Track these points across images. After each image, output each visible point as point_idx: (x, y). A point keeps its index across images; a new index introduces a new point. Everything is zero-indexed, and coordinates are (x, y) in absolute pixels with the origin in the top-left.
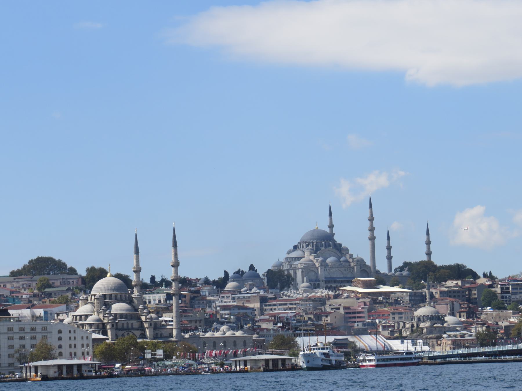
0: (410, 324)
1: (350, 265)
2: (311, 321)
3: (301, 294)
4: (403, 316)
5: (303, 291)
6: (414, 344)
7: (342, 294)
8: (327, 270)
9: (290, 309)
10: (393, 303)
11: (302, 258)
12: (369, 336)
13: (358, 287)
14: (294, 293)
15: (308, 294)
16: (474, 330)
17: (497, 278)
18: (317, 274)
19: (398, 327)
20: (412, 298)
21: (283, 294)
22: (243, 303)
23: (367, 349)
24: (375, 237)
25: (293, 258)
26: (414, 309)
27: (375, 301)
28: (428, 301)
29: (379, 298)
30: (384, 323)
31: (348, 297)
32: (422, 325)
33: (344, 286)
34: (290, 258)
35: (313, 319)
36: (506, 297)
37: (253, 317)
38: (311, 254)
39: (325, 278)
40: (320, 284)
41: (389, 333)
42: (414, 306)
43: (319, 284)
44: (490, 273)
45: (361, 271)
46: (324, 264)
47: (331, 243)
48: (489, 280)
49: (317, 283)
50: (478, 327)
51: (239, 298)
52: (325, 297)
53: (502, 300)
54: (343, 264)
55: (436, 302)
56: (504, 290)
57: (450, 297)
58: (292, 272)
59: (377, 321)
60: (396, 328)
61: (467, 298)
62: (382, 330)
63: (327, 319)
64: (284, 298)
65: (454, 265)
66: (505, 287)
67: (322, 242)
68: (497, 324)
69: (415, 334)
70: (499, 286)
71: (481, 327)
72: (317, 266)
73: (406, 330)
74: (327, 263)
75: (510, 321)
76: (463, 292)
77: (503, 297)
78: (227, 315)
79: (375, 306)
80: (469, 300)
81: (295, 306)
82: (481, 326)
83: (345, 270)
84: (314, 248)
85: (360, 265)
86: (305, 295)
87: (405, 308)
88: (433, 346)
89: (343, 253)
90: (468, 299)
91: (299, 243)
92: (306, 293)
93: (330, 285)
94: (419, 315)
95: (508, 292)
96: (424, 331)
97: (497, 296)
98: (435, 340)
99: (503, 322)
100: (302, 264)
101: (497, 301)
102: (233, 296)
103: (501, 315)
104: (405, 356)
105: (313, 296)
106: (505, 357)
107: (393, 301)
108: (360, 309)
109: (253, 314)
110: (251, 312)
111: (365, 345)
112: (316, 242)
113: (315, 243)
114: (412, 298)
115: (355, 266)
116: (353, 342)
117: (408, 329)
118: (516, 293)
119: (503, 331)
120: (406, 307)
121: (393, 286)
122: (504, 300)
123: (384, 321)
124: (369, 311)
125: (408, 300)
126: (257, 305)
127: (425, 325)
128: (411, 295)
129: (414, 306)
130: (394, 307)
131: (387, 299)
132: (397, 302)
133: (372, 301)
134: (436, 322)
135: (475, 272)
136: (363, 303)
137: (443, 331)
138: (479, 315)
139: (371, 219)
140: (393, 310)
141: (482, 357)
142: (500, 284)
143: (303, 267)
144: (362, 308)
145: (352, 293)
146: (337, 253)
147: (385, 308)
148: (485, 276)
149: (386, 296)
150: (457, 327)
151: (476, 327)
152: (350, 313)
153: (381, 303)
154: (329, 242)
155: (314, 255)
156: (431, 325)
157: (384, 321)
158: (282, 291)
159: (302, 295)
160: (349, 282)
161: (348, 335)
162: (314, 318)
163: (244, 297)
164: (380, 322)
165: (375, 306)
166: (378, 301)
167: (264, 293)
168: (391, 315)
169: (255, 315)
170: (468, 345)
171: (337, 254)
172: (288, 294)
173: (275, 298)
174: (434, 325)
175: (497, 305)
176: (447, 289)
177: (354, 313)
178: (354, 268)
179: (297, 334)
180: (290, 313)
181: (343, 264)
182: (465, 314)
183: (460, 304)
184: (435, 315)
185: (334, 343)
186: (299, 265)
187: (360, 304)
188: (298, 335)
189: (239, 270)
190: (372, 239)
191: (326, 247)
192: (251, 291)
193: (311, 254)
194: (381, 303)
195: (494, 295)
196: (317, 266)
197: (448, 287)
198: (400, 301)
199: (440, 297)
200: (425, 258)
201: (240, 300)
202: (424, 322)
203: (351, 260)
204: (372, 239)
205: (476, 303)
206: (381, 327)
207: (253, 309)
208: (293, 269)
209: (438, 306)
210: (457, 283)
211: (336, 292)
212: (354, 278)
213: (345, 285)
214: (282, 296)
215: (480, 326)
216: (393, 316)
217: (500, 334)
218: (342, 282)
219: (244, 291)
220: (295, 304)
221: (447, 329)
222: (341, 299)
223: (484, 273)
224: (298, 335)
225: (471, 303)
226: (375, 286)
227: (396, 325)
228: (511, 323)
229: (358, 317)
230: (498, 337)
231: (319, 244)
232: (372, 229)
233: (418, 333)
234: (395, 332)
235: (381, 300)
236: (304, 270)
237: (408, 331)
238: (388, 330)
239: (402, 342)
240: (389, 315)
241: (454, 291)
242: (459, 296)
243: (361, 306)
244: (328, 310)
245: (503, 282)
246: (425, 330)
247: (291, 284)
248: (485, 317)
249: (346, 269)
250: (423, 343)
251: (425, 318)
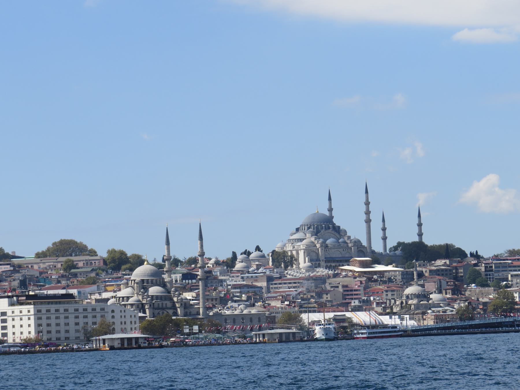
0: (400, 301)
1: (348, 246)
2: (313, 299)
3: (303, 274)
4: (395, 293)
5: (305, 271)
6: (402, 319)
7: (340, 274)
8: (327, 250)
9: (294, 287)
10: (387, 281)
11: (303, 239)
12: (364, 312)
13: (355, 266)
14: (297, 272)
15: (310, 273)
16: (458, 306)
17: (482, 258)
18: (318, 254)
19: (390, 304)
20: (404, 276)
21: (287, 273)
22: (252, 283)
23: (362, 324)
24: (371, 220)
25: (296, 239)
26: (405, 286)
27: (370, 280)
28: (416, 281)
29: (374, 276)
30: (378, 300)
31: (346, 276)
32: (410, 302)
33: (343, 266)
34: (293, 239)
35: (314, 297)
36: (490, 275)
37: (261, 294)
38: (312, 236)
39: (325, 258)
41: (382, 309)
42: (406, 284)
43: (319, 264)
44: (477, 252)
45: (358, 251)
46: (325, 246)
47: (331, 226)
48: (474, 260)
49: (318, 262)
50: (461, 303)
51: (248, 277)
52: (325, 276)
53: (486, 278)
54: (342, 245)
55: (426, 280)
56: (488, 268)
57: (439, 275)
58: (294, 253)
59: (372, 298)
60: (388, 305)
61: (454, 276)
62: (376, 307)
63: (327, 296)
64: (288, 277)
65: (444, 245)
66: (488, 266)
67: (322, 225)
68: (478, 300)
69: (404, 310)
70: (483, 265)
71: (463, 303)
72: (318, 247)
73: (397, 306)
74: (327, 244)
75: (489, 297)
76: (450, 270)
77: (486, 275)
78: (238, 293)
79: (370, 284)
80: (456, 278)
81: (299, 285)
82: (464, 302)
83: (343, 250)
84: (315, 230)
85: (357, 246)
86: (307, 274)
87: (397, 286)
88: (419, 320)
89: (342, 235)
90: (455, 277)
91: (301, 226)
92: (308, 272)
93: (329, 264)
94: (408, 294)
95: (492, 271)
96: (412, 307)
97: (481, 274)
98: (421, 315)
99: (483, 299)
100: (304, 246)
101: (480, 278)
102: (242, 275)
103: (483, 291)
104: (391, 330)
105: (314, 275)
106: (474, 330)
107: (387, 280)
108: (357, 287)
109: (261, 292)
110: (259, 291)
111: (360, 320)
112: (317, 225)
113: (316, 226)
114: (404, 276)
115: (352, 246)
116: (350, 318)
117: (398, 305)
118: (499, 271)
119: (481, 307)
120: (398, 284)
121: (387, 265)
122: (487, 278)
123: (378, 298)
124: (365, 289)
125: (401, 279)
126: (264, 284)
127: (413, 302)
128: (403, 273)
129: (406, 284)
130: (387, 285)
131: (381, 277)
132: (390, 280)
133: (367, 280)
134: (422, 299)
135: (464, 251)
136: (359, 282)
137: (429, 307)
138: (464, 292)
139: (367, 203)
140: (386, 288)
141: (455, 330)
142: (484, 263)
143: (304, 248)
144: (359, 286)
145: (350, 272)
147: (379, 285)
148: (472, 255)
149: (380, 275)
150: (440, 303)
151: (459, 303)
152: (348, 291)
153: (376, 281)
154: (328, 225)
155: (315, 237)
156: (418, 302)
157: (378, 298)
158: (286, 271)
159: (304, 274)
160: (347, 261)
161: (346, 312)
162: (316, 296)
163: (252, 277)
164: (374, 299)
165: (370, 284)
166: (373, 279)
167: (270, 272)
168: (384, 292)
169: (263, 293)
170: (449, 319)
171: (336, 236)
172: (292, 274)
173: (280, 278)
174: (420, 302)
175: (481, 282)
176: (436, 268)
177: (351, 291)
178: (351, 249)
179: (302, 311)
180: (293, 292)
181: (342, 245)
182: (450, 291)
183: (447, 282)
184: (422, 293)
185: (333, 318)
186: (301, 246)
187: (357, 283)
188: (303, 312)
189: (246, 250)
190: (368, 221)
192: (258, 271)
193: (312, 236)
194: (376, 281)
195: (479, 273)
196: (318, 247)
197: (437, 266)
198: (393, 279)
199: (430, 275)
201: (249, 279)
202: (412, 299)
203: (349, 242)
204: (368, 221)
205: (462, 280)
206: (375, 303)
207: (261, 288)
208: (295, 250)
209: (427, 283)
210: (446, 262)
211: (335, 271)
212: (352, 257)
213: (344, 264)
214: (286, 275)
215: (462, 302)
216: (387, 293)
217: (479, 309)
218: (341, 261)
219: (252, 271)
220: (299, 283)
221: (432, 306)
222: (340, 278)
223: (471, 252)
224: (303, 312)
225: (458, 281)
226: (371, 266)
227: (388, 302)
228: (490, 299)
229: (355, 295)
230: (475, 312)
231: (320, 226)
232: (368, 213)
233: (407, 309)
234: (387, 308)
235: (376, 278)
237: (398, 308)
238: (381, 306)
239: (391, 318)
240: (383, 292)
241: (443, 270)
242: (446, 274)
243: (357, 284)
244: (328, 288)
245: (487, 262)
246: (413, 307)
247: (294, 264)
248: (469, 293)
249: (344, 250)
250: (409, 318)
251: (412, 296)
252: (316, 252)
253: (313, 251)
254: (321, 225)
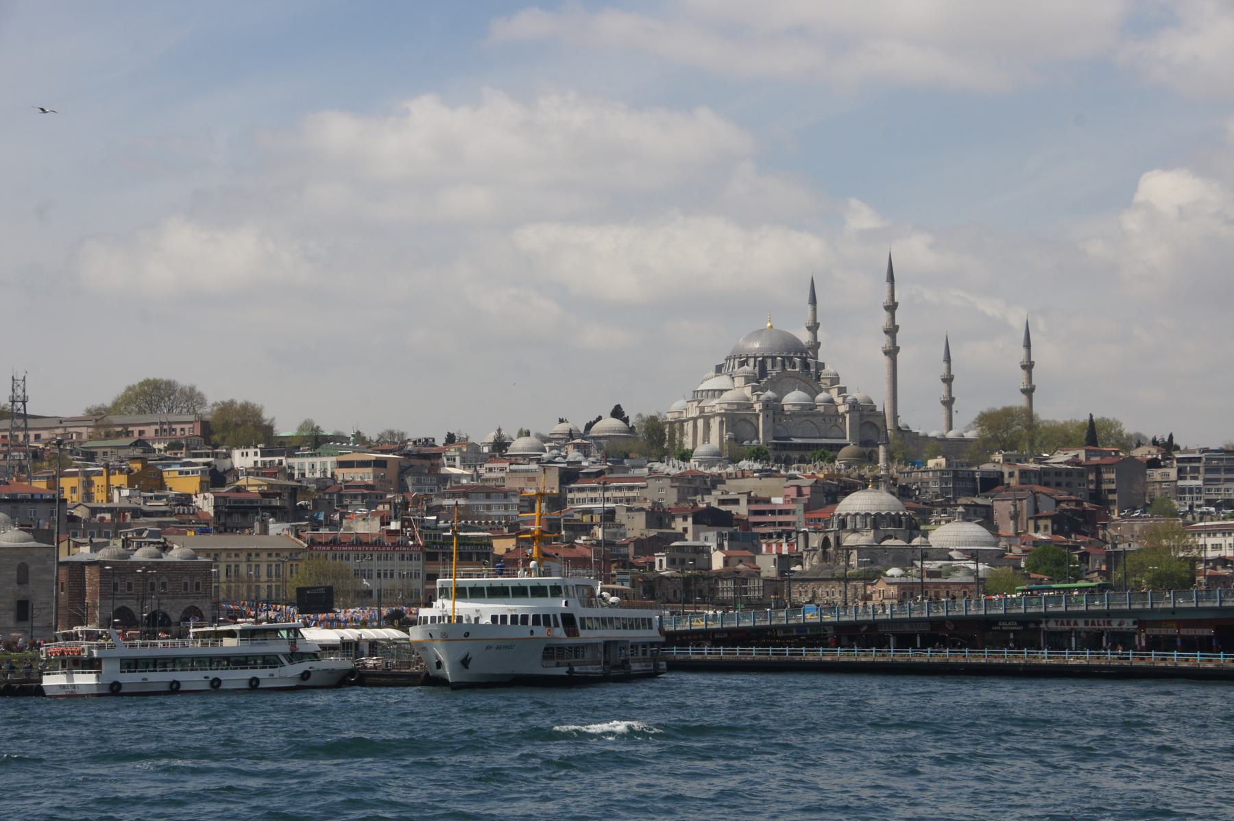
83: (824, 420)
113: (760, 359)
143: (723, 411)
155: (753, 387)
178: (845, 418)
196: (757, 411)
200: (1020, 401)
203: (839, 400)
236: (724, 419)
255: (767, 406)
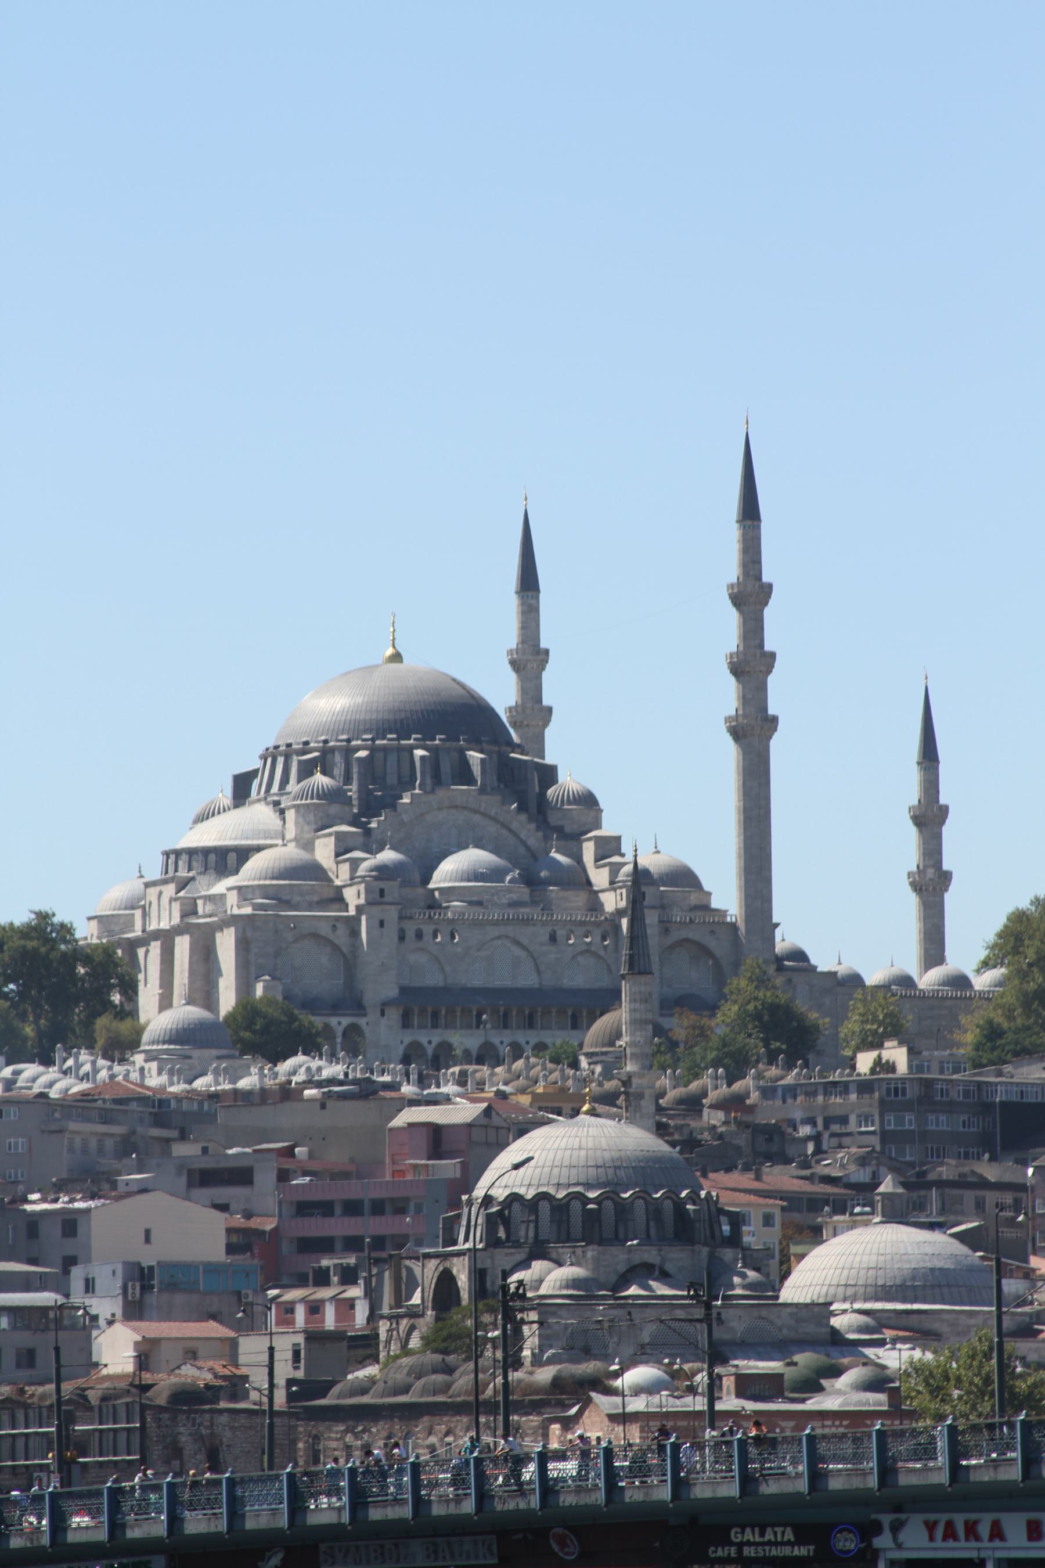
8: (419, 935)
40: (367, 1030)
49: (346, 1021)
83: (553, 938)
93: (436, 1040)
112: (373, 750)
113: (362, 754)
146: (515, 826)
155: (339, 837)
171: (516, 835)
178: (618, 927)
191: (436, 777)
252: (335, 947)
253: (315, 936)
254: (400, 749)
255: (382, 892)
